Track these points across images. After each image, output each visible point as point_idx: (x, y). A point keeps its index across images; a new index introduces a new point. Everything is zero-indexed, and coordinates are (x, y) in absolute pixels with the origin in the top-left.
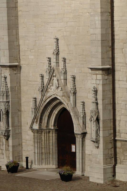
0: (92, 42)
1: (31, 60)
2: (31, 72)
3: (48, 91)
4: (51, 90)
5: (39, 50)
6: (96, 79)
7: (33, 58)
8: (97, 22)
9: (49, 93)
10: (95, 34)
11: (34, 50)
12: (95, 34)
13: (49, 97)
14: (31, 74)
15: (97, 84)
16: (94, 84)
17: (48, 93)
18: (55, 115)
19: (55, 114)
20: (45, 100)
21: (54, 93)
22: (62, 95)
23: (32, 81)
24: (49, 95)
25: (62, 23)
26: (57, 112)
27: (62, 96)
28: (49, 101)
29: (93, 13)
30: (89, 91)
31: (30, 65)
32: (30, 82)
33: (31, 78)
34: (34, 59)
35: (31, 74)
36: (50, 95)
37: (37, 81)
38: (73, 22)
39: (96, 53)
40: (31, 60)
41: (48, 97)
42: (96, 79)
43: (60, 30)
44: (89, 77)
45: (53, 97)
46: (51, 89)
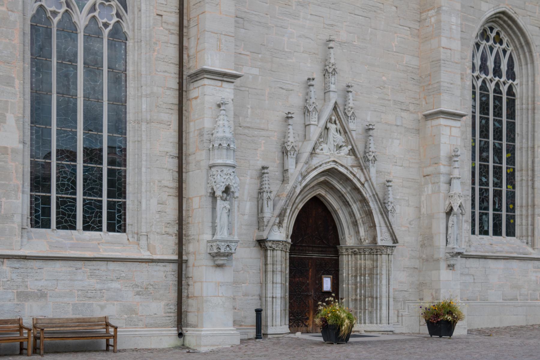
0: (445, 63)
1: (251, 77)
2: (249, 106)
3: (316, 154)
4: (321, 151)
5: (274, 58)
6: (450, 136)
7: (258, 74)
8: (454, 27)
9: (316, 158)
10: (450, 49)
11: (260, 56)
12: (450, 49)
13: (316, 168)
14: (249, 111)
15: (451, 145)
16: (445, 143)
17: (315, 156)
18: (299, 211)
19: (298, 209)
20: (306, 173)
21: (330, 158)
22: (350, 165)
23: (253, 128)
24: (318, 161)
25: (338, 12)
26: (303, 205)
27: (352, 166)
28: (341, 173)
29: (447, 8)
30: (396, 162)
31: (247, 89)
32: (246, 131)
33: (248, 120)
34: (260, 77)
35: (249, 111)
36: (320, 163)
37: (267, 130)
38: (361, 17)
39: (452, 86)
40: (251, 77)
41: (314, 167)
42: (449, 134)
43: (332, 25)
44: (396, 134)
45: (328, 167)
46: (322, 150)
